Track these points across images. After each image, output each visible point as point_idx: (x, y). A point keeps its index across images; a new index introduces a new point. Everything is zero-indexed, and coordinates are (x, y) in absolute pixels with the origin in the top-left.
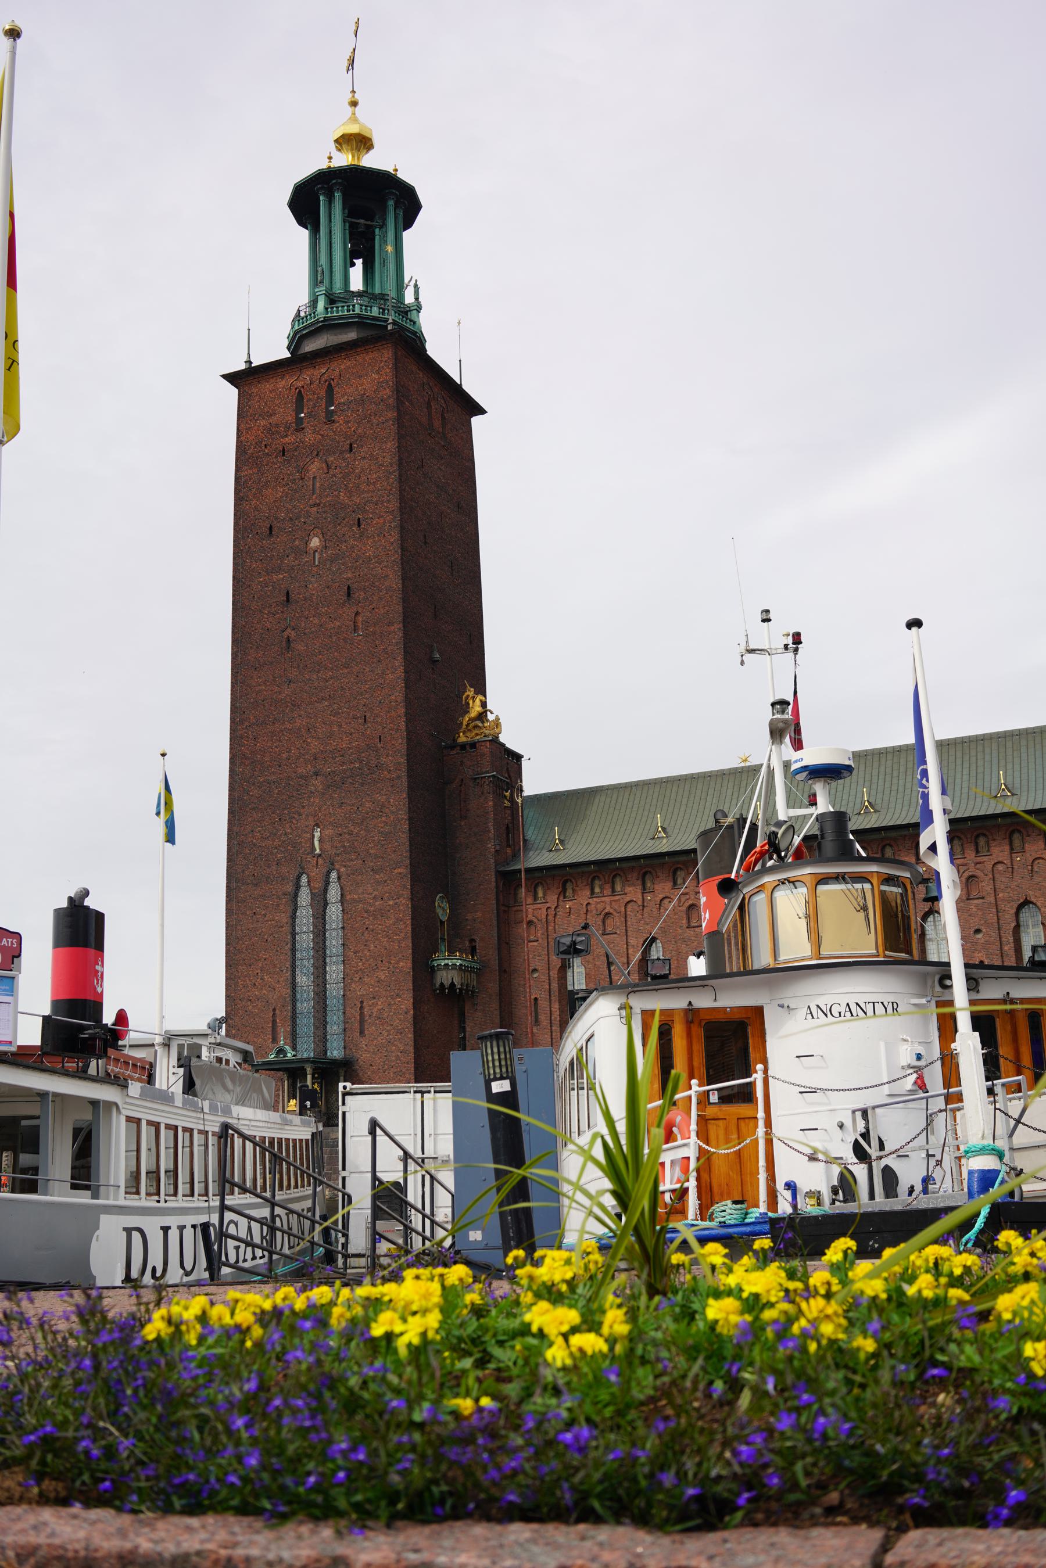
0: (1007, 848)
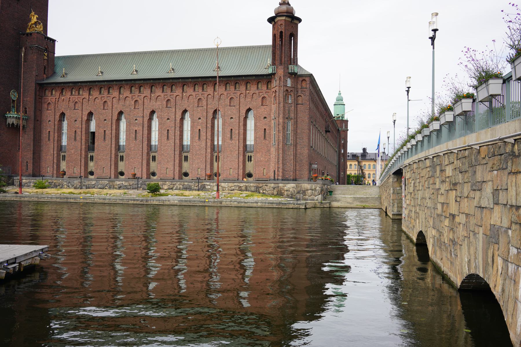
0: (213, 89)
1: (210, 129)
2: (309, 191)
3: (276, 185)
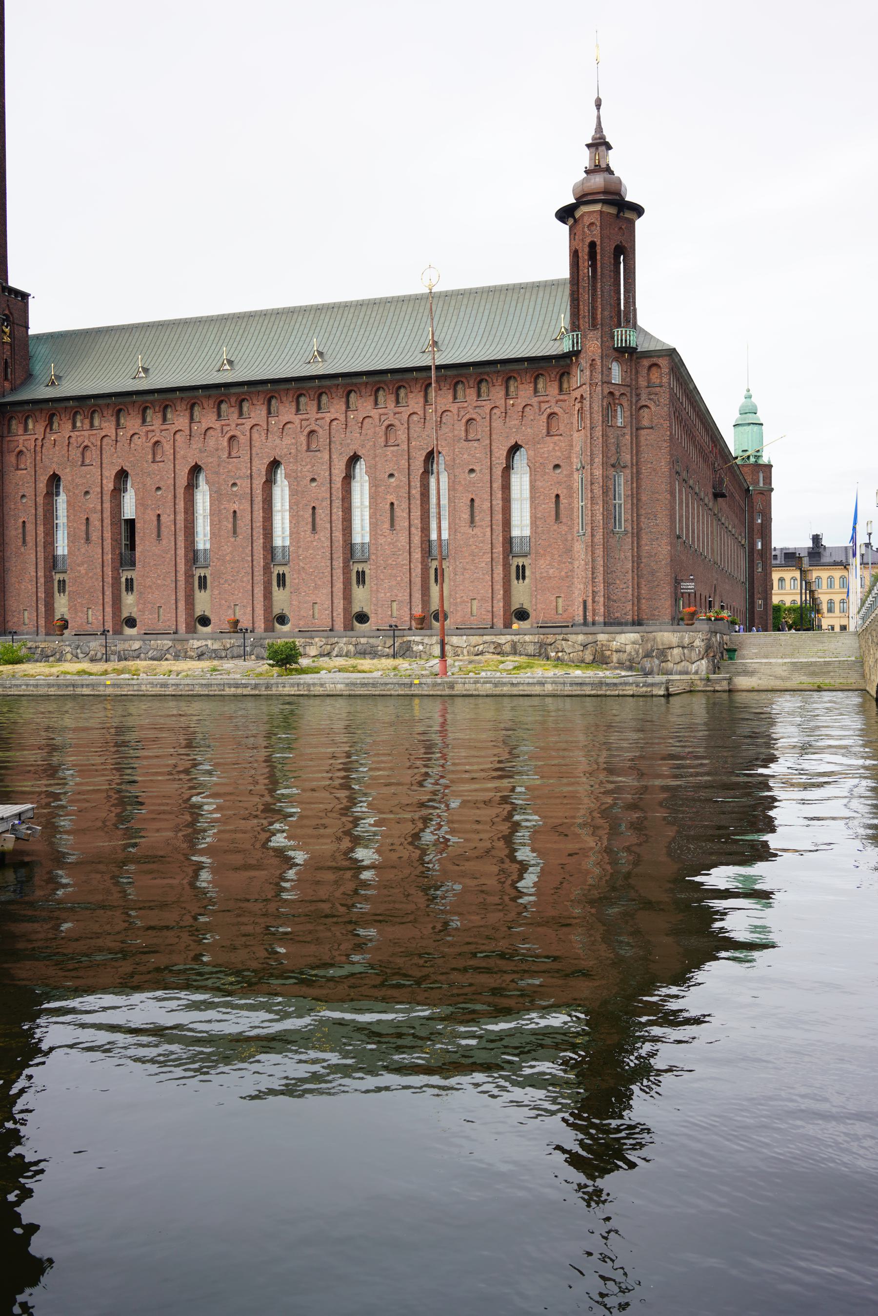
0: (422, 400)
1: (419, 502)
2: (676, 651)
3: (591, 638)
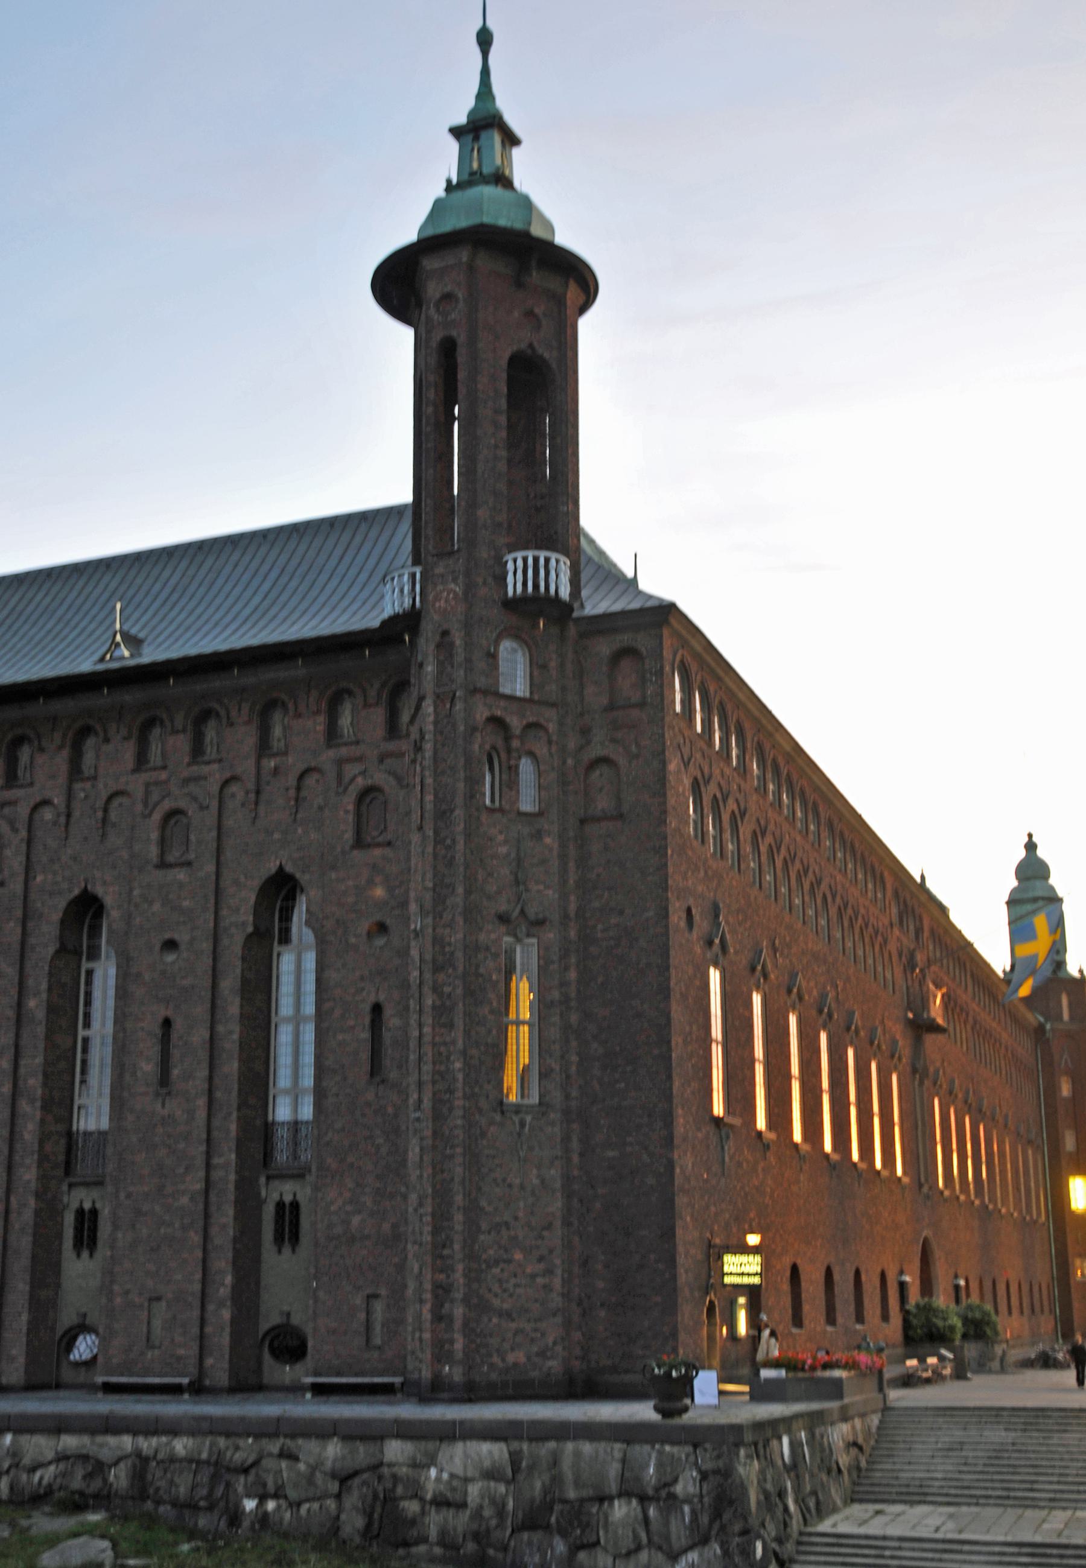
1: (41, 1030)
2: (620, 1510)
3: (363, 1453)
